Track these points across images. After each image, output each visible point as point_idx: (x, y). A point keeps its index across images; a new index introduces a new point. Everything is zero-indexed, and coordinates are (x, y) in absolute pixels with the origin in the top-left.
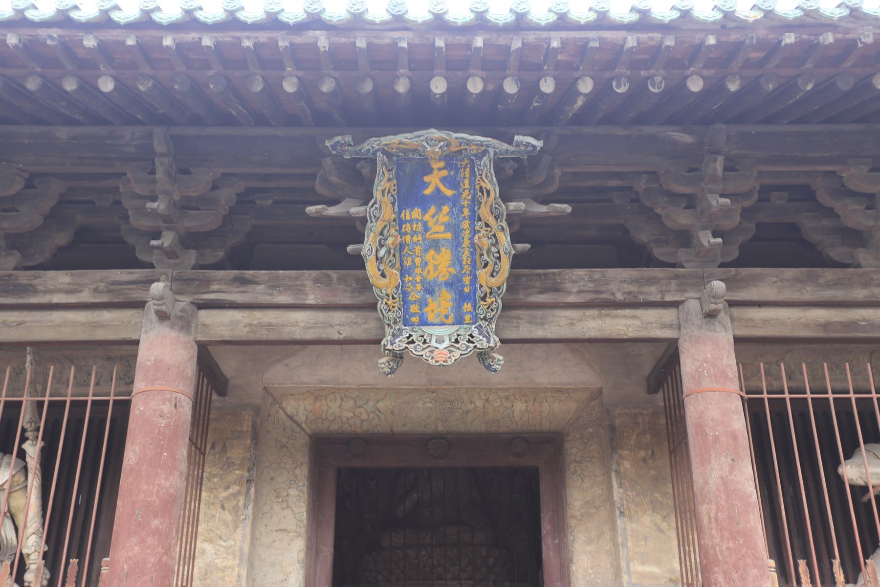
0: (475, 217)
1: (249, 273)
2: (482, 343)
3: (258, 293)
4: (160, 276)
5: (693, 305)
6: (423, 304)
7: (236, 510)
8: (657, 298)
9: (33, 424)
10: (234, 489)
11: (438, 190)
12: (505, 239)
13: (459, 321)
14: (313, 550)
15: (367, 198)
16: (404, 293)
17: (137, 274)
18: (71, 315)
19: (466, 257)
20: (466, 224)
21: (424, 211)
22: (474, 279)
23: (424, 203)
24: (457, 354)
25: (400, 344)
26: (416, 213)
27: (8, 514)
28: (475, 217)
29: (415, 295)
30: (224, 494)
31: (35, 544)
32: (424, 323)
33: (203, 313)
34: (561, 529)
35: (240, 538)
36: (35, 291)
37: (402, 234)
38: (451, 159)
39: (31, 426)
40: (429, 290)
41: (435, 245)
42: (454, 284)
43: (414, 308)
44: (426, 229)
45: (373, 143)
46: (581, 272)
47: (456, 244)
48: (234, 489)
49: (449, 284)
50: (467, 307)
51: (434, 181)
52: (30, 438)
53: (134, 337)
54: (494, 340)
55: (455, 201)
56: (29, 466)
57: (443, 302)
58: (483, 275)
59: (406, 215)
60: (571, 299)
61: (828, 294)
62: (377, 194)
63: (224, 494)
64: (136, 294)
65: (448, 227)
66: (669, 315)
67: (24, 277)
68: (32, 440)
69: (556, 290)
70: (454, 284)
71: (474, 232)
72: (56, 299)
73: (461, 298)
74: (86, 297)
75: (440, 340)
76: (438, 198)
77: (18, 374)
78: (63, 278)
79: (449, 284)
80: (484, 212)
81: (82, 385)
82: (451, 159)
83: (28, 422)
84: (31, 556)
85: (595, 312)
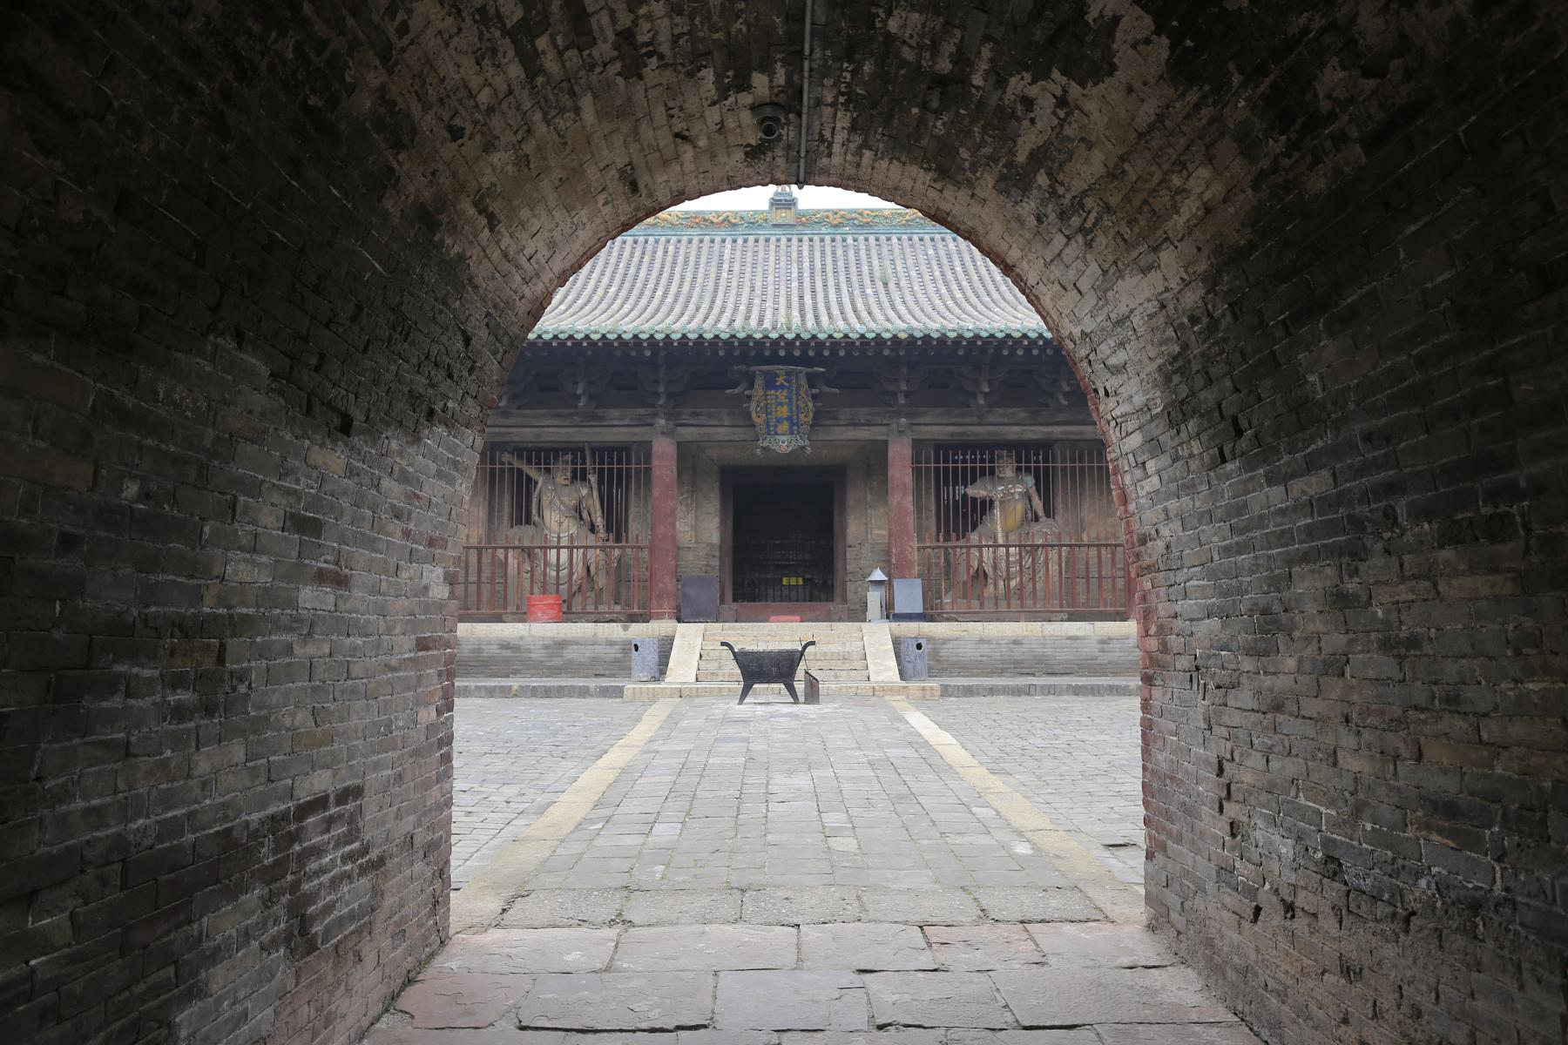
0: (798, 394)
1: (698, 410)
2: (801, 443)
3: (702, 420)
5: (894, 426)
6: (776, 427)
7: (687, 505)
8: (879, 422)
10: (686, 495)
11: (782, 384)
12: (810, 405)
13: (792, 433)
14: (723, 522)
15: (751, 386)
16: (768, 422)
17: (650, 410)
18: (622, 429)
19: (794, 408)
20: (794, 397)
21: (776, 391)
22: (798, 417)
23: (776, 388)
24: (790, 449)
25: (766, 444)
26: (773, 392)
28: (798, 394)
29: (772, 424)
30: (681, 498)
32: (776, 434)
33: (679, 428)
34: (843, 512)
35: (690, 518)
37: (766, 400)
38: (787, 373)
40: (779, 421)
41: (781, 404)
42: (789, 419)
43: (772, 428)
44: (777, 397)
45: (755, 368)
46: (846, 410)
47: (790, 404)
48: (686, 495)
49: (787, 419)
50: (795, 428)
51: (780, 380)
54: (807, 442)
55: (789, 388)
57: (786, 425)
58: (802, 416)
59: (768, 392)
60: (842, 423)
61: (954, 420)
62: (756, 386)
63: (681, 498)
64: (649, 421)
65: (786, 397)
66: (884, 429)
67: (599, 412)
69: (835, 418)
70: (789, 419)
71: (798, 400)
72: (615, 423)
73: (792, 424)
74: (627, 422)
75: (783, 442)
76: (782, 387)
78: (615, 413)
79: (787, 419)
80: (802, 393)
82: (787, 373)
85: (851, 428)
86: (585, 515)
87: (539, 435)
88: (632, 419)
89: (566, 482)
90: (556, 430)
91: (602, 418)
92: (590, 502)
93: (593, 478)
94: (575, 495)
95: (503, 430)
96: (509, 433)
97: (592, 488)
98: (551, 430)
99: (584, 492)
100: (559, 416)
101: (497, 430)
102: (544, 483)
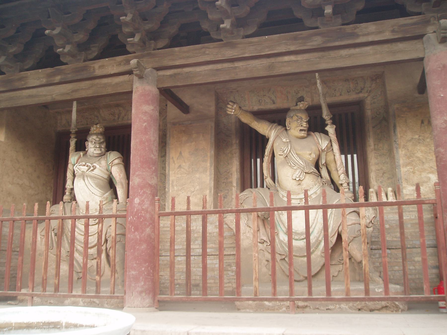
4: (430, 18)
9: (329, 116)
27: (325, 164)
31: (344, 178)
36: (358, 36)
39: (328, 117)
52: (329, 124)
53: (421, 56)
56: (332, 139)
67: (349, 28)
68: (330, 125)
74: (387, 35)
77: (297, 94)
78: (371, 27)
81: (332, 96)
83: (326, 116)
84: (343, 185)
86: (324, 172)
87: (271, 67)
88: (393, 31)
89: (303, 134)
90: (292, 58)
91: (354, 35)
92: (330, 157)
93: (331, 129)
94: (314, 148)
95: (226, 65)
96: (235, 68)
97: (331, 141)
98: (286, 58)
99: (324, 144)
100: (295, 38)
101: (219, 66)
102: (277, 136)
